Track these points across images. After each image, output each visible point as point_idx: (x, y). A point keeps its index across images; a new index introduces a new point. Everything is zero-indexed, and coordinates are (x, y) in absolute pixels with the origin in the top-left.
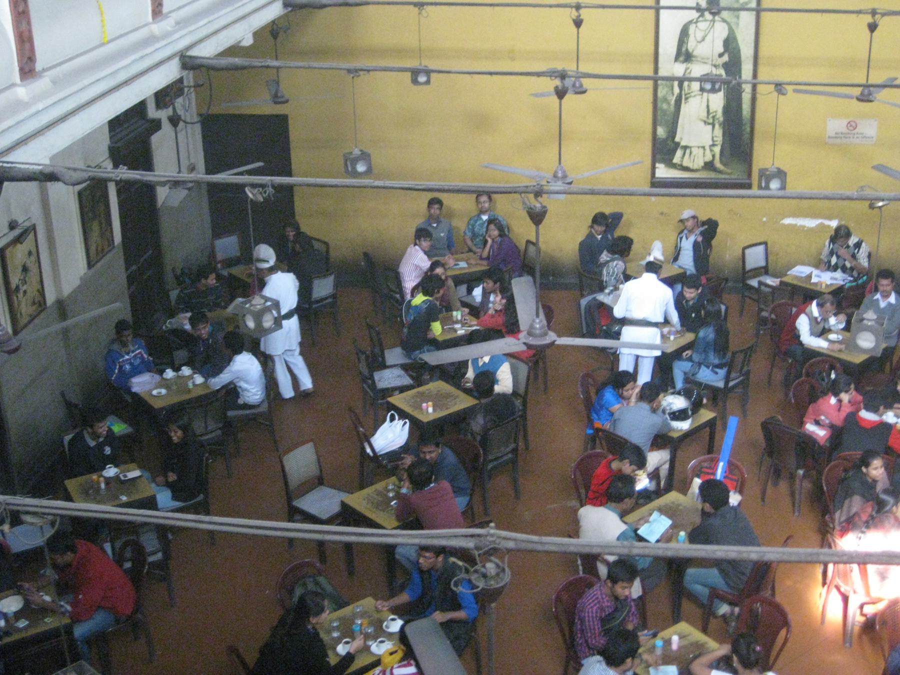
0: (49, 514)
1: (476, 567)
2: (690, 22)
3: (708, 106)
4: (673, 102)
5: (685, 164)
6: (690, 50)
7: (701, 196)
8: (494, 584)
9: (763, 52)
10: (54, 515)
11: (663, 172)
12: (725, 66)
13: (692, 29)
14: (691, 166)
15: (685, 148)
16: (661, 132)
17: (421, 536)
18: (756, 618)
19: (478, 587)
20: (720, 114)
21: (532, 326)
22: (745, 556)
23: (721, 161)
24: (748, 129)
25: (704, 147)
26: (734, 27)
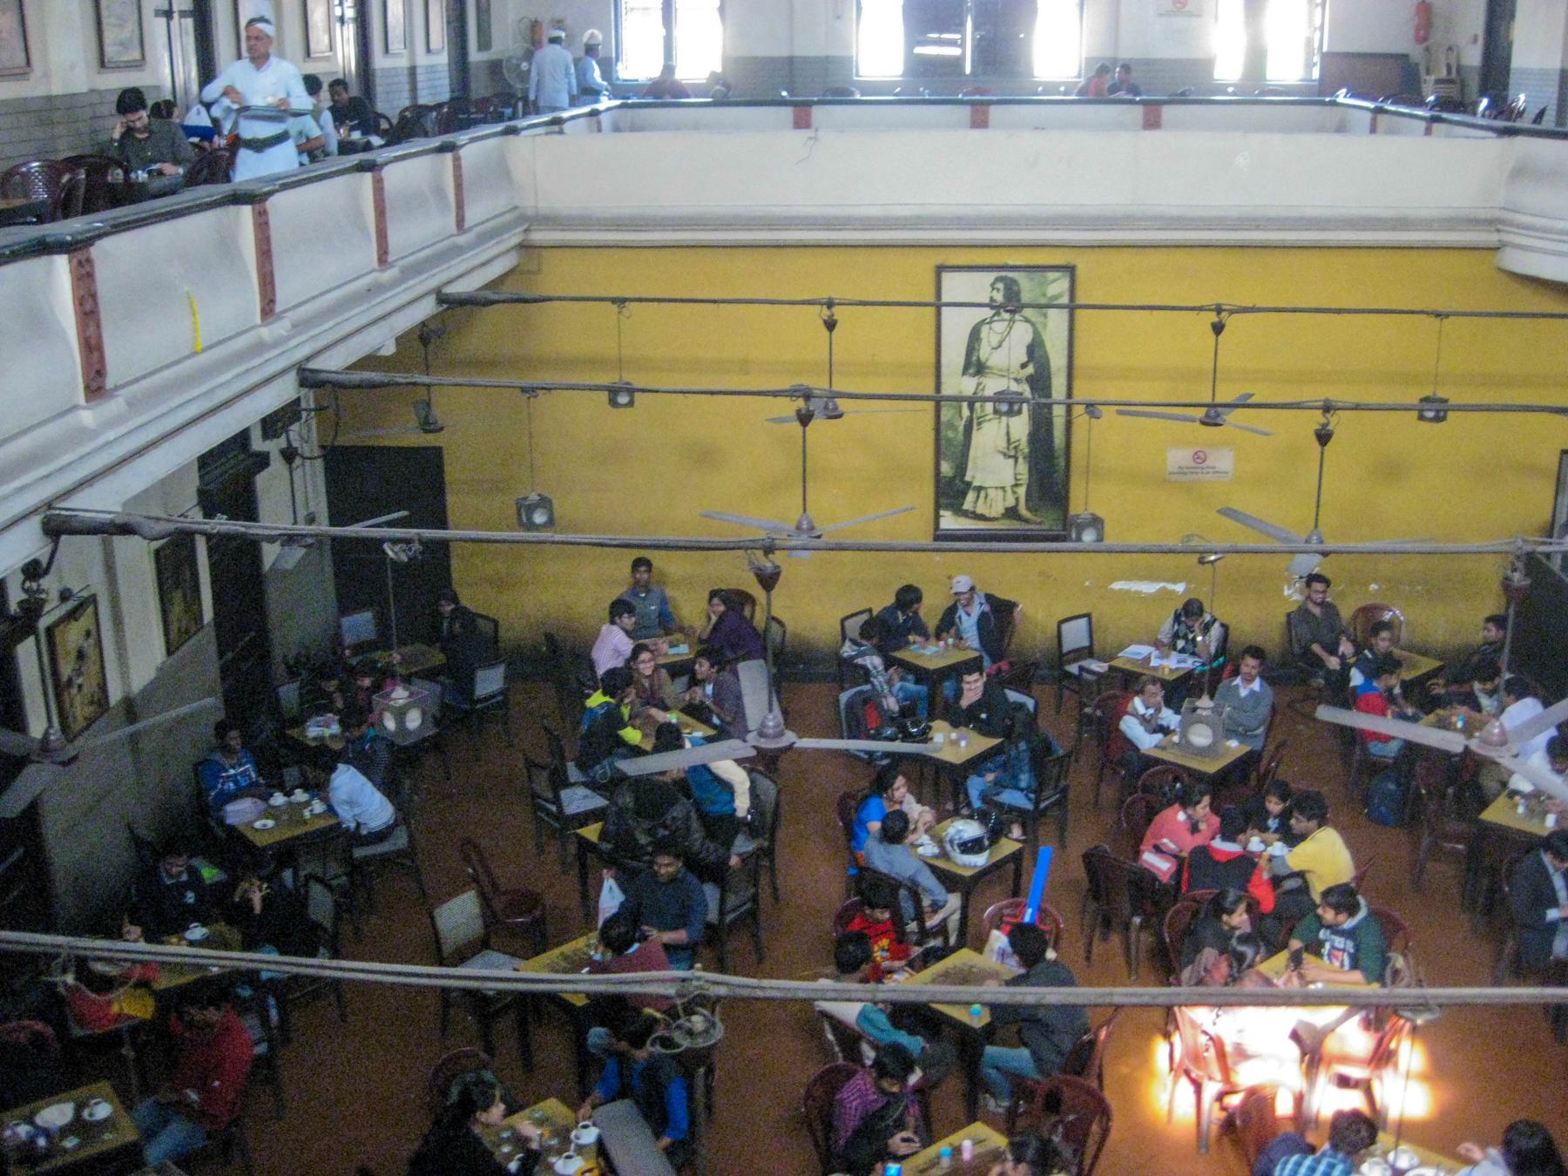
0: (125, 960)
1: (680, 1022)
2: (983, 322)
3: (1008, 434)
4: (961, 428)
5: (979, 511)
6: (983, 357)
7: (958, 550)
8: (701, 1043)
9: (1077, 362)
10: (134, 962)
11: (949, 521)
12: (1031, 380)
13: (985, 330)
14: (987, 513)
15: (979, 489)
16: (946, 468)
17: (607, 982)
18: (1060, 1099)
19: (679, 1046)
20: (1024, 446)
21: (763, 725)
22: (1019, 999)
23: (1028, 508)
24: (1062, 462)
25: (1003, 488)
26: (1040, 328)
